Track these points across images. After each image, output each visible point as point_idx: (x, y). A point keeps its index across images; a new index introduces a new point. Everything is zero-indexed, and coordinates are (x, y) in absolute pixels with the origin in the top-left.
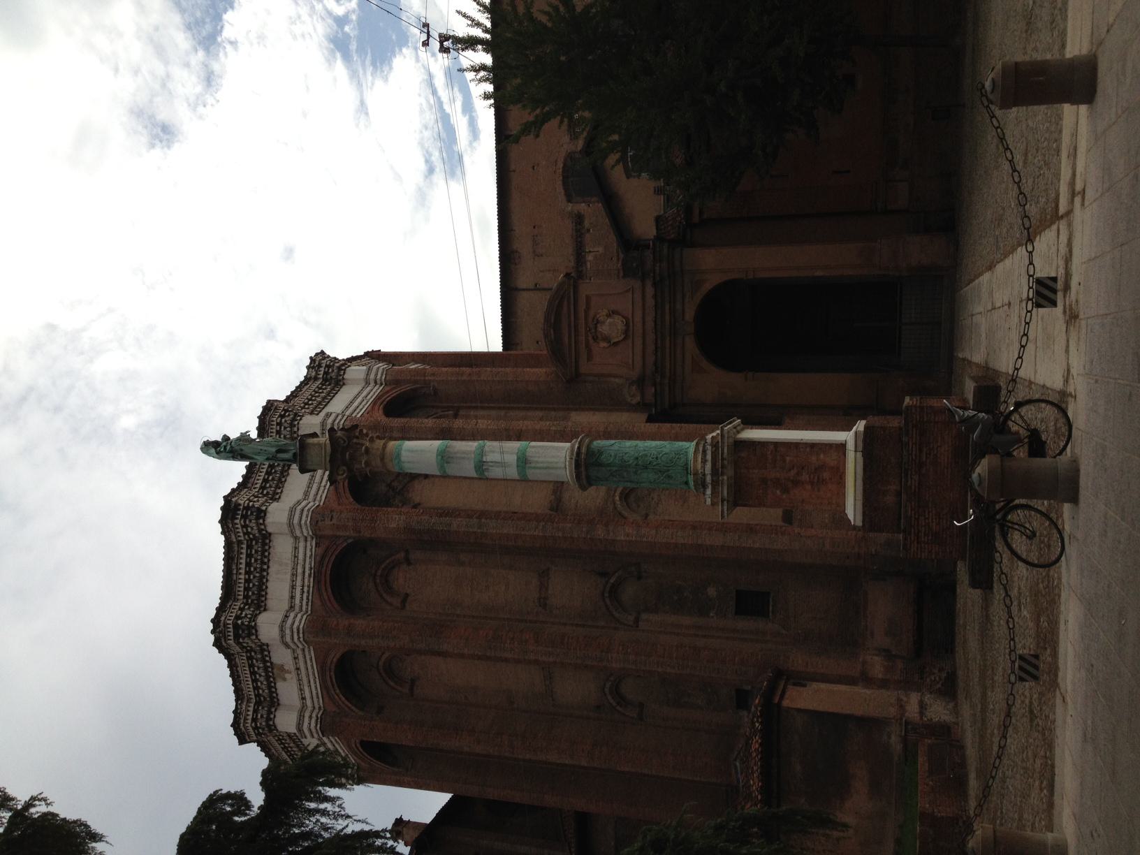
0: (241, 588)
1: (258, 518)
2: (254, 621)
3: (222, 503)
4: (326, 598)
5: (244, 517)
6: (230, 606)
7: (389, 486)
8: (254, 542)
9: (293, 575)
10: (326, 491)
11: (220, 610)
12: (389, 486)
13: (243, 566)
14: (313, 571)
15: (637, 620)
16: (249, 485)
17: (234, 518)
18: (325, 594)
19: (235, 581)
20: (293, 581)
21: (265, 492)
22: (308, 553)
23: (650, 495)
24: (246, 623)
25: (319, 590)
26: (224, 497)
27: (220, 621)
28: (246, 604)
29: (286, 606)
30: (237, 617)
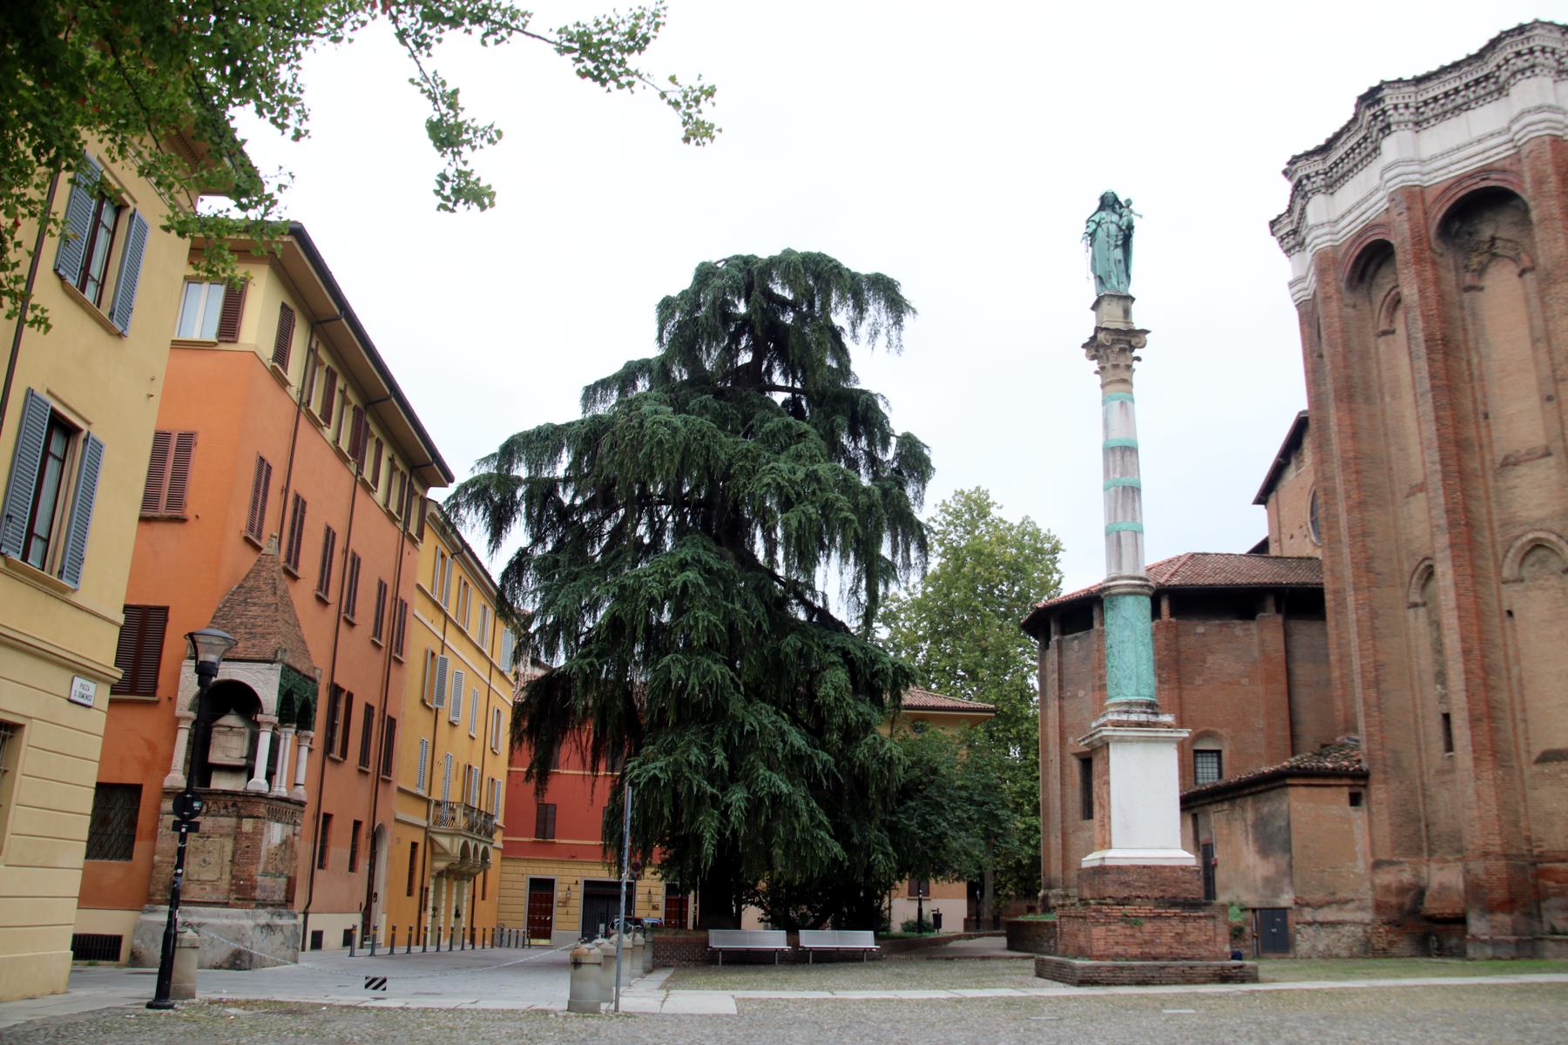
0: (1335, 156)
1: (1381, 130)
3: (1376, 83)
5: (1375, 117)
7: (1493, 239)
11: (1308, 155)
12: (1493, 239)
15: (1415, 605)
17: (1368, 107)
21: (1422, 110)
25: (1354, 241)
29: (1334, 217)
30: (1308, 177)
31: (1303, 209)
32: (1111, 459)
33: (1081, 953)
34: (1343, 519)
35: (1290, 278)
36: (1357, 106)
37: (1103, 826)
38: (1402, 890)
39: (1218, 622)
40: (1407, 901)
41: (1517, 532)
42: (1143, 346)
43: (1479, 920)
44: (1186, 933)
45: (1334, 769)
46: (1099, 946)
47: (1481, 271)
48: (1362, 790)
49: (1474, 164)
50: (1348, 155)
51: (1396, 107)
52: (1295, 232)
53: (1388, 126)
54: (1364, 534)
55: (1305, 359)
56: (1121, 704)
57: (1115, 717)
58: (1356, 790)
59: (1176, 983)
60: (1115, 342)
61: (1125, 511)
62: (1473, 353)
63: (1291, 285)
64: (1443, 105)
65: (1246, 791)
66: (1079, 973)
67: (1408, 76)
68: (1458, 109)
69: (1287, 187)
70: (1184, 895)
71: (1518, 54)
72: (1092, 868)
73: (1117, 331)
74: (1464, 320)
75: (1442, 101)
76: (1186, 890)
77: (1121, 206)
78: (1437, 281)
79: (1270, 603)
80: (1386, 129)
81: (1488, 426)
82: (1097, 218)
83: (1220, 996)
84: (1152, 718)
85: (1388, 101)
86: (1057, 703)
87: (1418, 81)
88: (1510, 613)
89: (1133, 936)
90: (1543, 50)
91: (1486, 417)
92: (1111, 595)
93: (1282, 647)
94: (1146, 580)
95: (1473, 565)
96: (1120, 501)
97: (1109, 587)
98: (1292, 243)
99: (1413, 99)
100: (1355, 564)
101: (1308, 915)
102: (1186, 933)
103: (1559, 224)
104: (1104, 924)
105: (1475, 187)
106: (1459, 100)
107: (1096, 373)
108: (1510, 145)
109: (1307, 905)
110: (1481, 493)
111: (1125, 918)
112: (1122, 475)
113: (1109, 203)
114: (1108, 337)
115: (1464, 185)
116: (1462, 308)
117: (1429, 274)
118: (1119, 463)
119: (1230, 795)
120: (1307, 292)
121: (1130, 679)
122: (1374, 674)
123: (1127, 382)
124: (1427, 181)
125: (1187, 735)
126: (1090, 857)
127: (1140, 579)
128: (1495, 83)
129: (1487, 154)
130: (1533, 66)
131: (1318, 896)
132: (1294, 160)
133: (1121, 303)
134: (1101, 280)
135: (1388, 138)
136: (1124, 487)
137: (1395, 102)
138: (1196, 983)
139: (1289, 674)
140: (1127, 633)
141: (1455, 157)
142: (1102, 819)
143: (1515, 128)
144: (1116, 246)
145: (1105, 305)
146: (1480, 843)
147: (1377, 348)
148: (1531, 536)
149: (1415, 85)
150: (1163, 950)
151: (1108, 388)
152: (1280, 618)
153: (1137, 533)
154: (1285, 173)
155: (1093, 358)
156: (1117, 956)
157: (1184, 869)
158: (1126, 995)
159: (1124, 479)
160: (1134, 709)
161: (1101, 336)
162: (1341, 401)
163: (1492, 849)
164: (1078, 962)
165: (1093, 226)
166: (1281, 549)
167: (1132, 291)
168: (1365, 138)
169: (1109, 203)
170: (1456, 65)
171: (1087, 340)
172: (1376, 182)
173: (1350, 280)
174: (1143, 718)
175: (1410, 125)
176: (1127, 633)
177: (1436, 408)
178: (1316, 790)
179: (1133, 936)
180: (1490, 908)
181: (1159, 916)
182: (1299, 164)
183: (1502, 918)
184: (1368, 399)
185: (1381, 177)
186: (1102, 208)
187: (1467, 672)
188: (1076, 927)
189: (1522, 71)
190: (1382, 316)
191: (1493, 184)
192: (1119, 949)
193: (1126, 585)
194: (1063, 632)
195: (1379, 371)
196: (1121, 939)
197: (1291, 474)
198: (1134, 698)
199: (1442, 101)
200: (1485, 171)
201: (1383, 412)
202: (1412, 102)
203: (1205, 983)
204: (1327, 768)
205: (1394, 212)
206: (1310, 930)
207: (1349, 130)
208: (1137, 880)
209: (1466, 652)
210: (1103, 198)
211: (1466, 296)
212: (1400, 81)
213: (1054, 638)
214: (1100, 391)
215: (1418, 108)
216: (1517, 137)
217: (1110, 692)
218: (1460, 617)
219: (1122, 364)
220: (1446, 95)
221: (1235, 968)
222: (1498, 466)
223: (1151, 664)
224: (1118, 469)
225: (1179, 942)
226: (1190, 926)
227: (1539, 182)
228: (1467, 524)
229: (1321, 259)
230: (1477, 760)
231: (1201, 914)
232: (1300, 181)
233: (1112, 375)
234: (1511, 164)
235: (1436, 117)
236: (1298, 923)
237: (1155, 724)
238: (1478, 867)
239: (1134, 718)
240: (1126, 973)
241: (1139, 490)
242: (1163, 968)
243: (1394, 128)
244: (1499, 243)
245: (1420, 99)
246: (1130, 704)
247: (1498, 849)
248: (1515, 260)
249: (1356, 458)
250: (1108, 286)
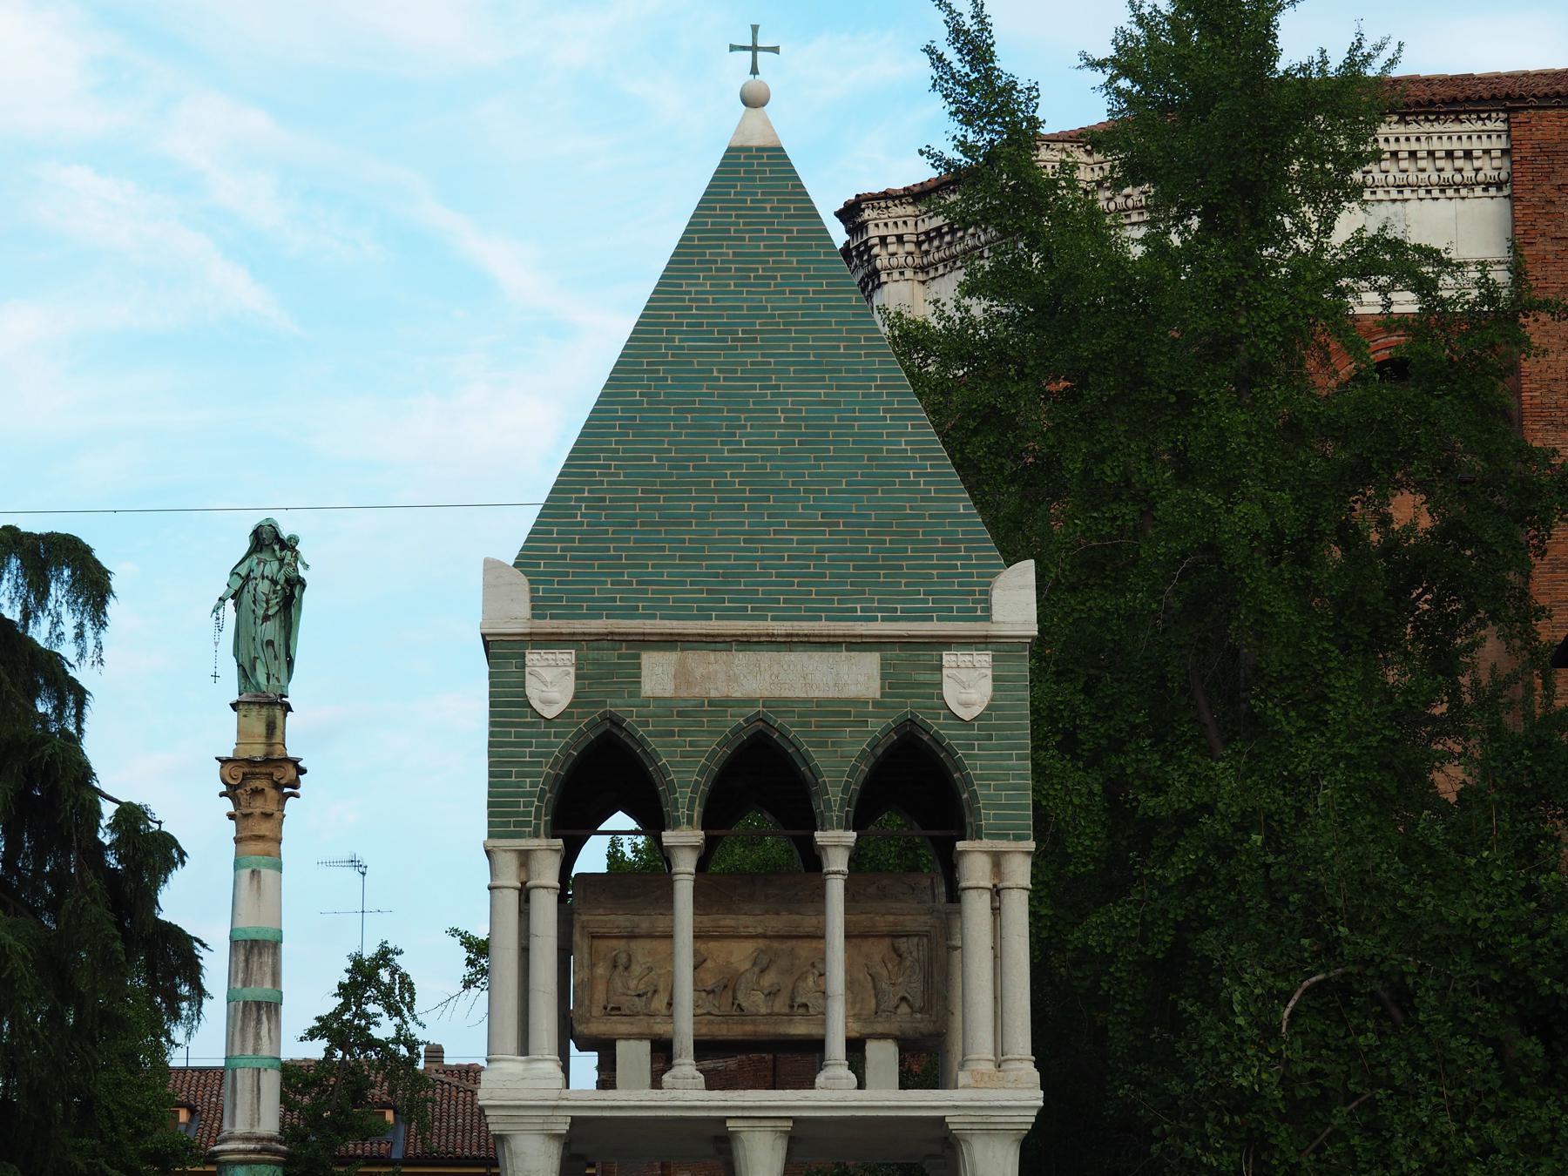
51: (883, 240)
85: (872, 231)
99: (911, 228)
112: (244, 985)
113: (267, 540)
136: (246, 1003)
137: (883, 232)
144: (266, 618)
159: (245, 990)
169: (267, 540)
175: (909, 273)
202: (908, 231)
210: (257, 534)
212: (886, 195)
215: (919, 244)
243: (884, 277)
245: (922, 228)
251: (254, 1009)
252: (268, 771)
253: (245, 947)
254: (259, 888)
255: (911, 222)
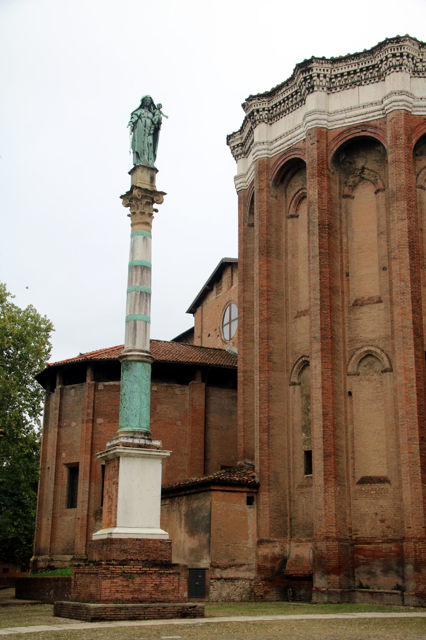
1: (308, 89)
2: (259, 122)
3: (309, 58)
4: (278, 164)
5: (305, 79)
6: (264, 101)
8: (377, 69)
9: (287, 133)
10: (341, 126)
11: (260, 96)
12: (363, 168)
13: (286, 95)
14: (291, 145)
15: (294, 384)
16: (335, 65)
17: (302, 72)
18: (280, 162)
19: (278, 95)
20: (284, 135)
22: (298, 137)
23: (375, 372)
24: (256, 119)
25: (281, 157)
26: (313, 57)
27: (251, 100)
28: (269, 111)
29: (270, 140)
30: (258, 111)
31: (251, 131)
32: (134, 273)
33: (92, 599)
34: (257, 327)
35: (236, 174)
36: (295, 70)
37: (110, 512)
38: (274, 559)
39: (165, 384)
40: (277, 565)
41: (358, 346)
42: (161, 203)
43: (321, 579)
44: (161, 584)
45: (239, 481)
46: (106, 593)
47: (354, 187)
48: (255, 496)
49: (359, 120)
50: (284, 101)
51: (318, 76)
52: (243, 145)
53: (313, 87)
54: (268, 338)
55: (239, 226)
56: (128, 432)
57: (125, 440)
58: (251, 495)
59: (154, 619)
60: (143, 197)
61: (140, 308)
62: (344, 236)
63: (236, 178)
64: (346, 79)
65: (183, 493)
66: (92, 613)
67: (328, 57)
68: (354, 84)
69: (242, 115)
70: (160, 559)
71: (394, 56)
72: (102, 540)
73: (146, 190)
74: (341, 215)
75: (346, 77)
76: (162, 556)
77: (155, 108)
78: (329, 189)
79: (199, 375)
80: (311, 89)
81: (348, 280)
82: (138, 113)
83: (191, 626)
84: (148, 442)
85: (314, 71)
86: (56, 430)
87: (334, 61)
88: (350, 393)
89: (127, 586)
90: (408, 56)
91: (348, 275)
92: (127, 360)
93: (204, 403)
94: (150, 353)
95: (333, 363)
96: (138, 301)
97: (127, 356)
98: (240, 151)
99: (329, 72)
100: (261, 356)
101: (218, 573)
102: (161, 584)
103: (403, 165)
104: (110, 578)
105: (358, 135)
106: (356, 78)
107: (129, 215)
108: (381, 112)
109: (218, 567)
110: (340, 320)
111: (124, 574)
112: (141, 284)
114: (140, 193)
115: (352, 132)
116: (340, 207)
117: (325, 184)
118: (139, 276)
119: (171, 495)
120: (245, 184)
121: (136, 416)
122: (267, 424)
123: (148, 224)
124: (330, 126)
125: (169, 454)
126: (99, 532)
127: (147, 352)
128: (377, 71)
129: (367, 116)
130: (402, 65)
131: (224, 561)
132: (251, 98)
133: (149, 172)
134: (137, 155)
135: (311, 95)
137: (318, 72)
138: (167, 618)
139: (206, 420)
140: (136, 386)
141: (349, 114)
142: (110, 507)
143: (385, 102)
144: (149, 134)
145: (139, 172)
146: (325, 531)
147: (286, 225)
148: (366, 349)
149: (332, 64)
150: (147, 595)
151: (136, 227)
152: (203, 385)
153: (147, 322)
154: (243, 106)
155: (127, 206)
156: (117, 601)
157: (161, 541)
158: (129, 627)
159: (141, 287)
160: (136, 436)
161: (135, 192)
162: (263, 255)
163: (331, 535)
164: (92, 605)
165: (136, 118)
166: (202, 343)
167: (156, 165)
168: (296, 92)
170: (357, 55)
171: (124, 193)
172: (299, 121)
173: (275, 181)
174: (142, 442)
175: (325, 89)
176: (136, 386)
177: (321, 266)
178: (228, 494)
179: (127, 586)
180: (327, 572)
181: (145, 573)
182: (254, 101)
183: (334, 578)
184: (278, 256)
185: (304, 119)
186: (142, 106)
187: (325, 426)
188: (88, 580)
189: (395, 67)
190: (292, 206)
191: (369, 134)
192: (118, 595)
193: (138, 355)
194: (65, 383)
195: (286, 240)
196: (120, 589)
197: (212, 297)
198: (137, 429)
199: (346, 77)
200: (365, 126)
201: (286, 265)
203: (172, 618)
204: (235, 480)
205: (308, 143)
206: (219, 583)
207: (287, 85)
208: (132, 548)
209: (325, 415)
211: (344, 201)
212: (323, 58)
213: (58, 387)
214: (130, 228)
215: (331, 79)
216: (386, 108)
217: (121, 423)
218: (323, 393)
219: (147, 212)
220: (349, 73)
221: (190, 608)
222: (351, 305)
223: (149, 407)
224: (139, 280)
225: (156, 590)
226: (164, 579)
227: (396, 138)
228: (332, 338)
229: (260, 165)
230: (326, 480)
231: (171, 571)
232: (253, 113)
233: (139, 218)
234: (380, 124)
235: (341, 86)
236: (211, 579)
237: (149, 446)
238: (322, 546)
239: (136, 441)
240: (123, 612)
241: (150, 295)
242: (146, 608)
243: (315, 89)
244: (366, 172)
246: (134, 432)
247: (334, 535)
248: (374, 183)
249: (268, 291)
250: (142, 160)
251: (145, 295)
252: (152, 196)
253: (141, 268)
254: (147, 245)
255: (329, 71)
